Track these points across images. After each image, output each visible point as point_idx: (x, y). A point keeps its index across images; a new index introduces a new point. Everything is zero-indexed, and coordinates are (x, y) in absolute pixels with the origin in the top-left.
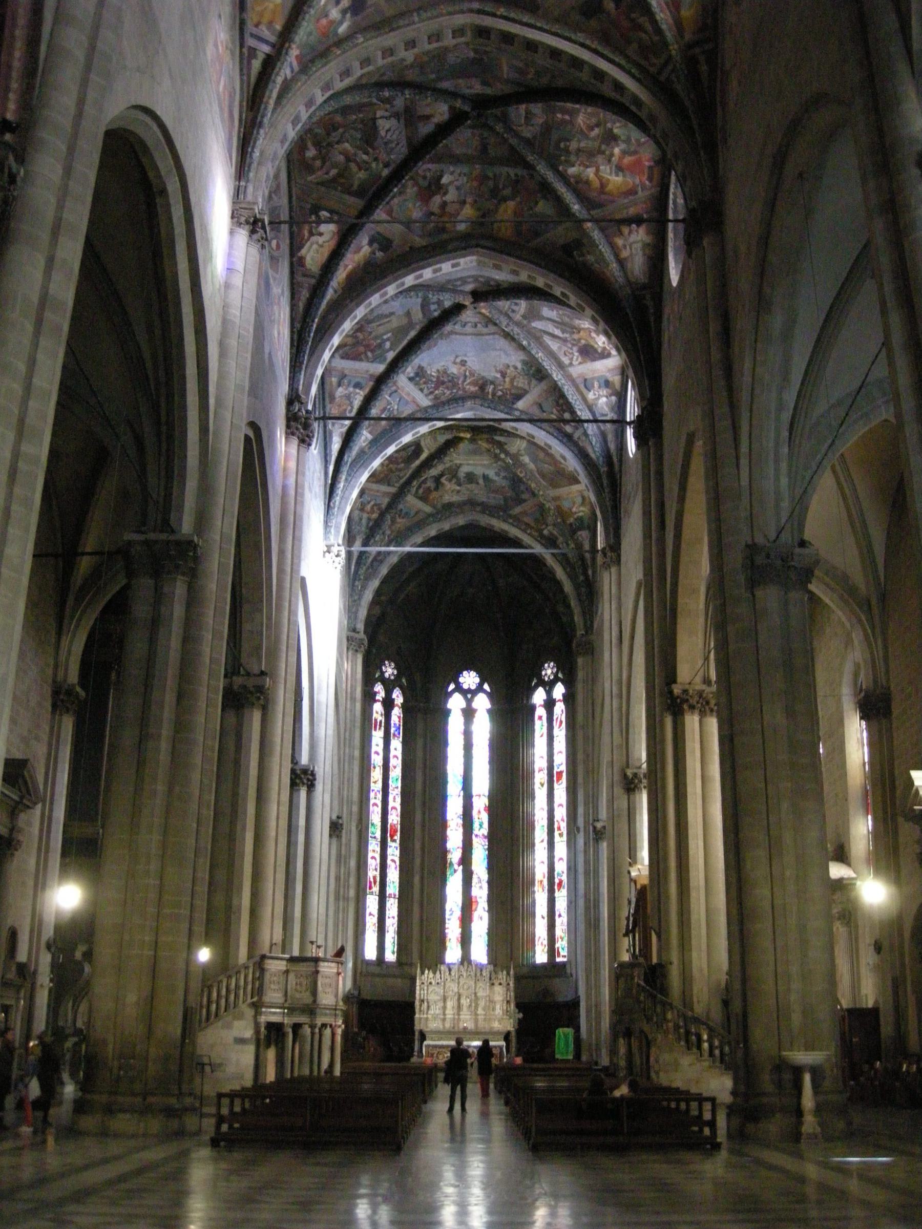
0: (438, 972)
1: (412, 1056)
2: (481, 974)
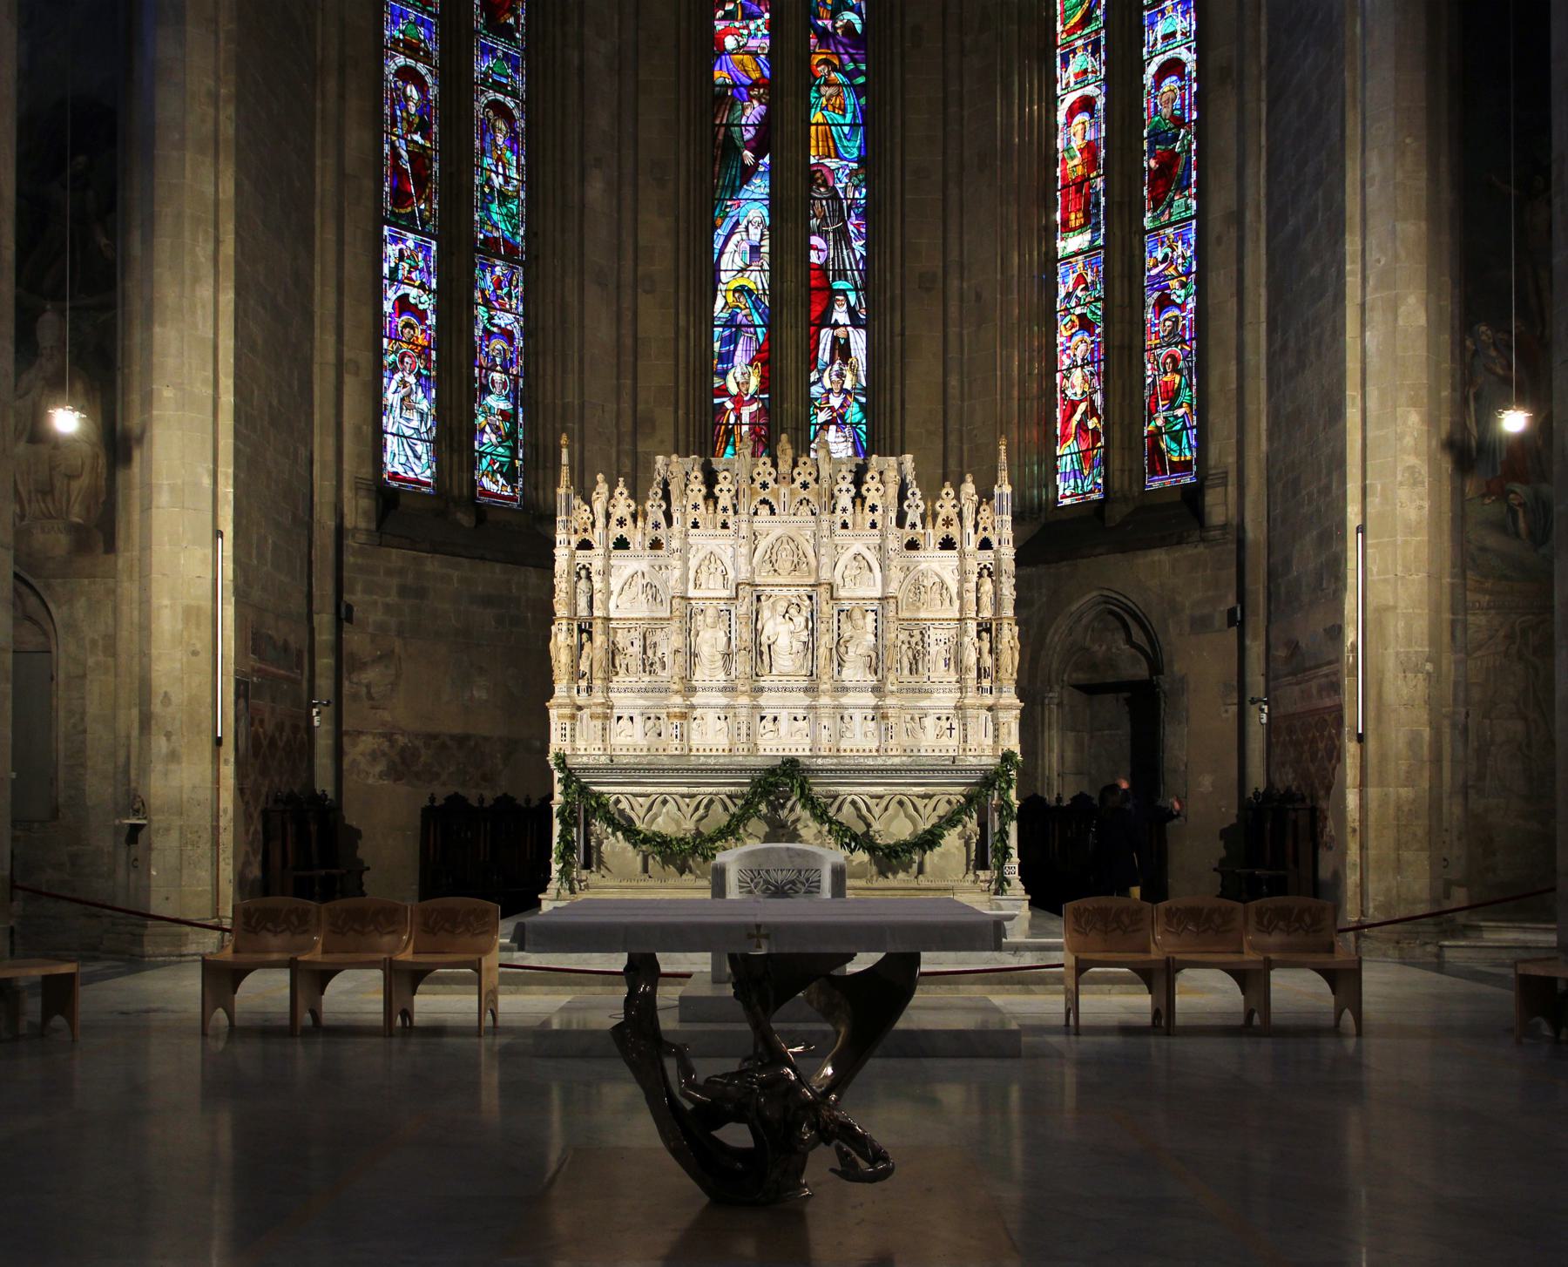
1: (542, 883)
2: (859, 498)
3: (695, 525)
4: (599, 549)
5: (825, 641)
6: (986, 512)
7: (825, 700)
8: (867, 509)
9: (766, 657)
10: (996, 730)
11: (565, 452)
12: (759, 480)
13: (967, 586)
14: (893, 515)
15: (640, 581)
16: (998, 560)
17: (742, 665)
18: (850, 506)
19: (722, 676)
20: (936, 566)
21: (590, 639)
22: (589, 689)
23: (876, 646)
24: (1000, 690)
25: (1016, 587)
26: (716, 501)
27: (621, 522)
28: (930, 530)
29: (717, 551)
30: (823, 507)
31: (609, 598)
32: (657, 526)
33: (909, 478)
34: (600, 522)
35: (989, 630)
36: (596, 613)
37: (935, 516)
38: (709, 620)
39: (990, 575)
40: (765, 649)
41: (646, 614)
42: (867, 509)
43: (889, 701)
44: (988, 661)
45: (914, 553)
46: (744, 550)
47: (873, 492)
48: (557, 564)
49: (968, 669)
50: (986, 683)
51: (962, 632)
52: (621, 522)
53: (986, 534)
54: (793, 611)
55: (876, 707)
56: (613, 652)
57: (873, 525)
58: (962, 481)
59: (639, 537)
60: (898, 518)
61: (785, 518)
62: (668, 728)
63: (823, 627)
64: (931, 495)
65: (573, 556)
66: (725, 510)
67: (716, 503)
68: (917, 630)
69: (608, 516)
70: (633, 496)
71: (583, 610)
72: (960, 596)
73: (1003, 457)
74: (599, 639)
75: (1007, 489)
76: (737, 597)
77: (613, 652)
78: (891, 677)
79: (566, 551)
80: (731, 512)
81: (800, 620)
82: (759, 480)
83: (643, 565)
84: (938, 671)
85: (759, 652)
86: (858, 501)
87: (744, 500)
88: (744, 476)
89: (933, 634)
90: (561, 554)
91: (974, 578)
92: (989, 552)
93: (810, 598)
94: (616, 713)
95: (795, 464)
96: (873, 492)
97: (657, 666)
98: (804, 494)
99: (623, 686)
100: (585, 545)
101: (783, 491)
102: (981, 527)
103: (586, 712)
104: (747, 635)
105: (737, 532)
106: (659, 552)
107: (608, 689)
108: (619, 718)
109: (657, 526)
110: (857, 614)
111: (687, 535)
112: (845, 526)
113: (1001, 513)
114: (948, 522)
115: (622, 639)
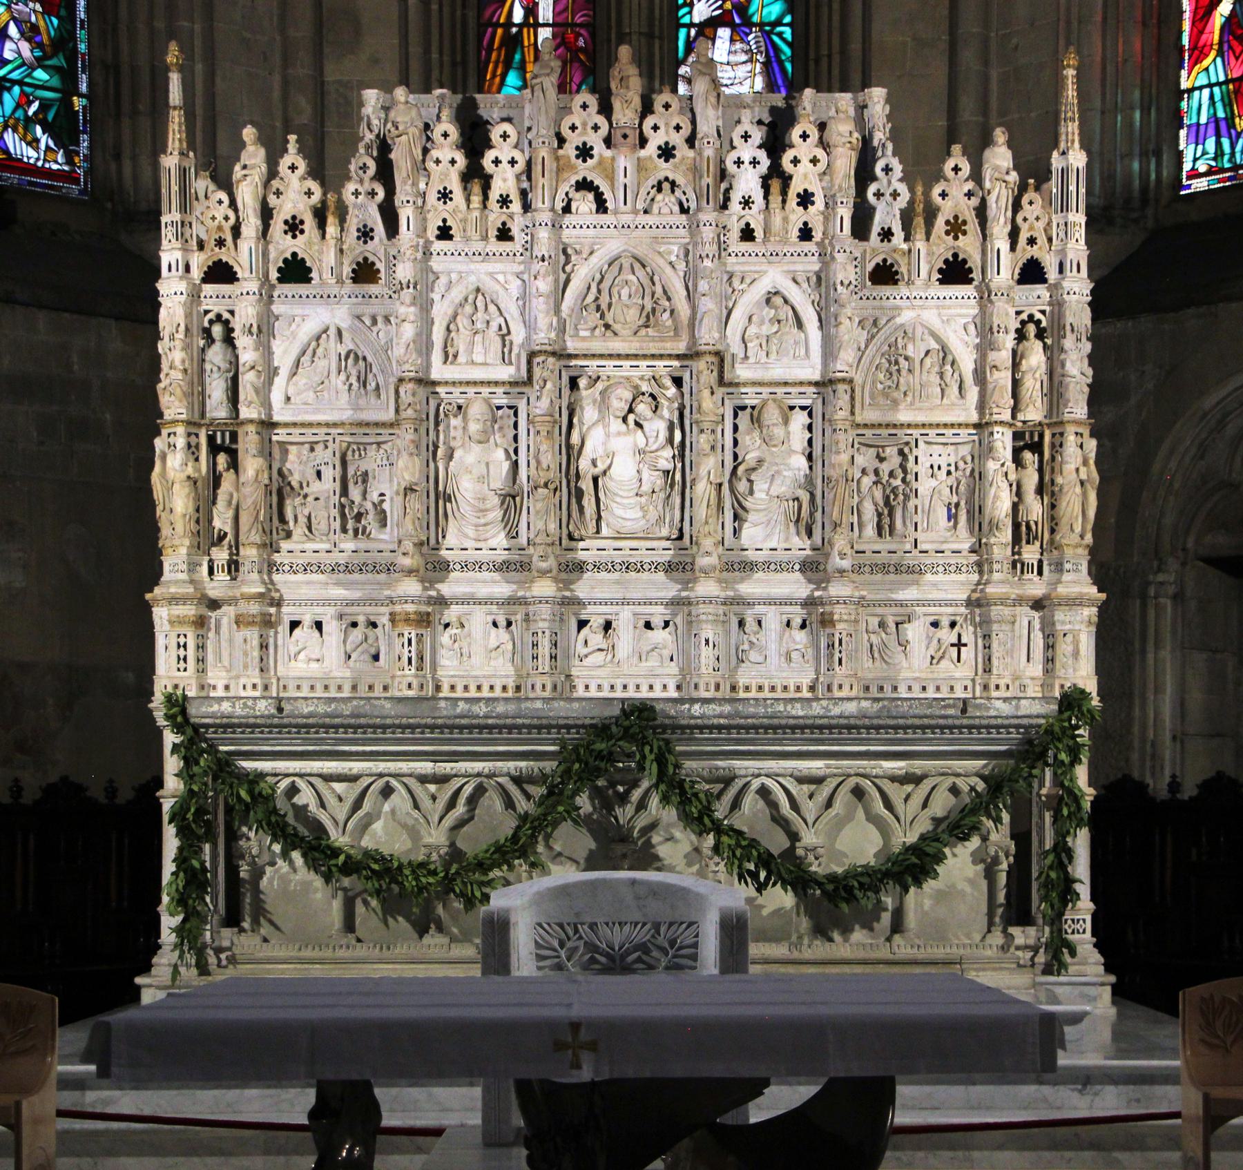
0: (363, 160)
3: (445, 233)
4: (249, 284)
5: (708, 469)
6: (1033, 207)
7: (706, 588)
8: (792, 201)
9: (589, 503)
10: (1049, 647)
11: (175, 80)
12: (574, 140)
13: (993, 357)
14: (845, 212)
15: (333, 348)
16: (1057, 305)
17: (540, 518)
18: (758, 195)
19: (500, 540)
20: (931, 317)
21: (234, 465)
22: (233, 566)
23: (809, 482)
24: (1059, 567)
25: (1093, 359)
26: (486, 181)
27: (294, 227)
28: (920, 244)
29: (488, 285)
30: (703, 196)
31: (270, 382)
32: (366, 234)
33: (879, 137)
34: (251, 226)
35: (1037, 448)
36: (245, 412)
37: (931, 214)
38: (474, 427)
39: (1040, 335)
40: (586, 485)
41: (347, 415)
42: (792, 201)
43: (837, 589)
44: (1035, 509)
45: (887, 290)
46: (544, 285)
47: (805, 165)
48: (163, 313)
49: (994, 526)
50: (1030, 554)
51: (984, 451)
52: (294, 227)
53: (1034, 251)
54: (643, 408)
55: (809, 603)
56: (280, 491)
57: (806, 234)
58: (986, 141)
59: (330, 257)
60: (854, 219)
61: (626, 219)
62: (396, 645)
63: (703, 441)
64: (923, 170)
65: (195, 296)
66: (504, 201)
67: (486, 188)
68: (892, 443)
69: (266, 214)
70: (317, 171)
71: (217, 408)
72: (980, 377)
73: (1071, 92)
74: (251, 465)
75: (1078, 159)
76: (529, 381)
77: (280, 491)
78: (840, 542)
79: (182, 286)
80: (516, 207)
81: (656, 427)
82: (574, 140)
83: (339, 315)
84: (935, 530)
85: (575, 490)
86: (775, 185)
87: (542, 182)
88: (544, 131)
89: (926, 456)
90: (172, 293)
91: (1009, 341)
92: (1041, 290)
93: (678, 382)
94: (289, 613)
95: (647, 108)
96: (805, 165)
97: (370, 520)
98: (665, 169)
99: (301, 560)
100: (221, 273)
101: (622, 162)
102: (1023, 236)
103: (228, 612)
104: (550, 458)
105: (528, 247)
106: (373, 289)
107: (271, 567)
108: (294, 625)
109: (366, 234)
110: (772, 415)
111: (427, 254)
112: (747, 234)
113: (1064, 208)
114: (956, 228)
115: (297, 465)
